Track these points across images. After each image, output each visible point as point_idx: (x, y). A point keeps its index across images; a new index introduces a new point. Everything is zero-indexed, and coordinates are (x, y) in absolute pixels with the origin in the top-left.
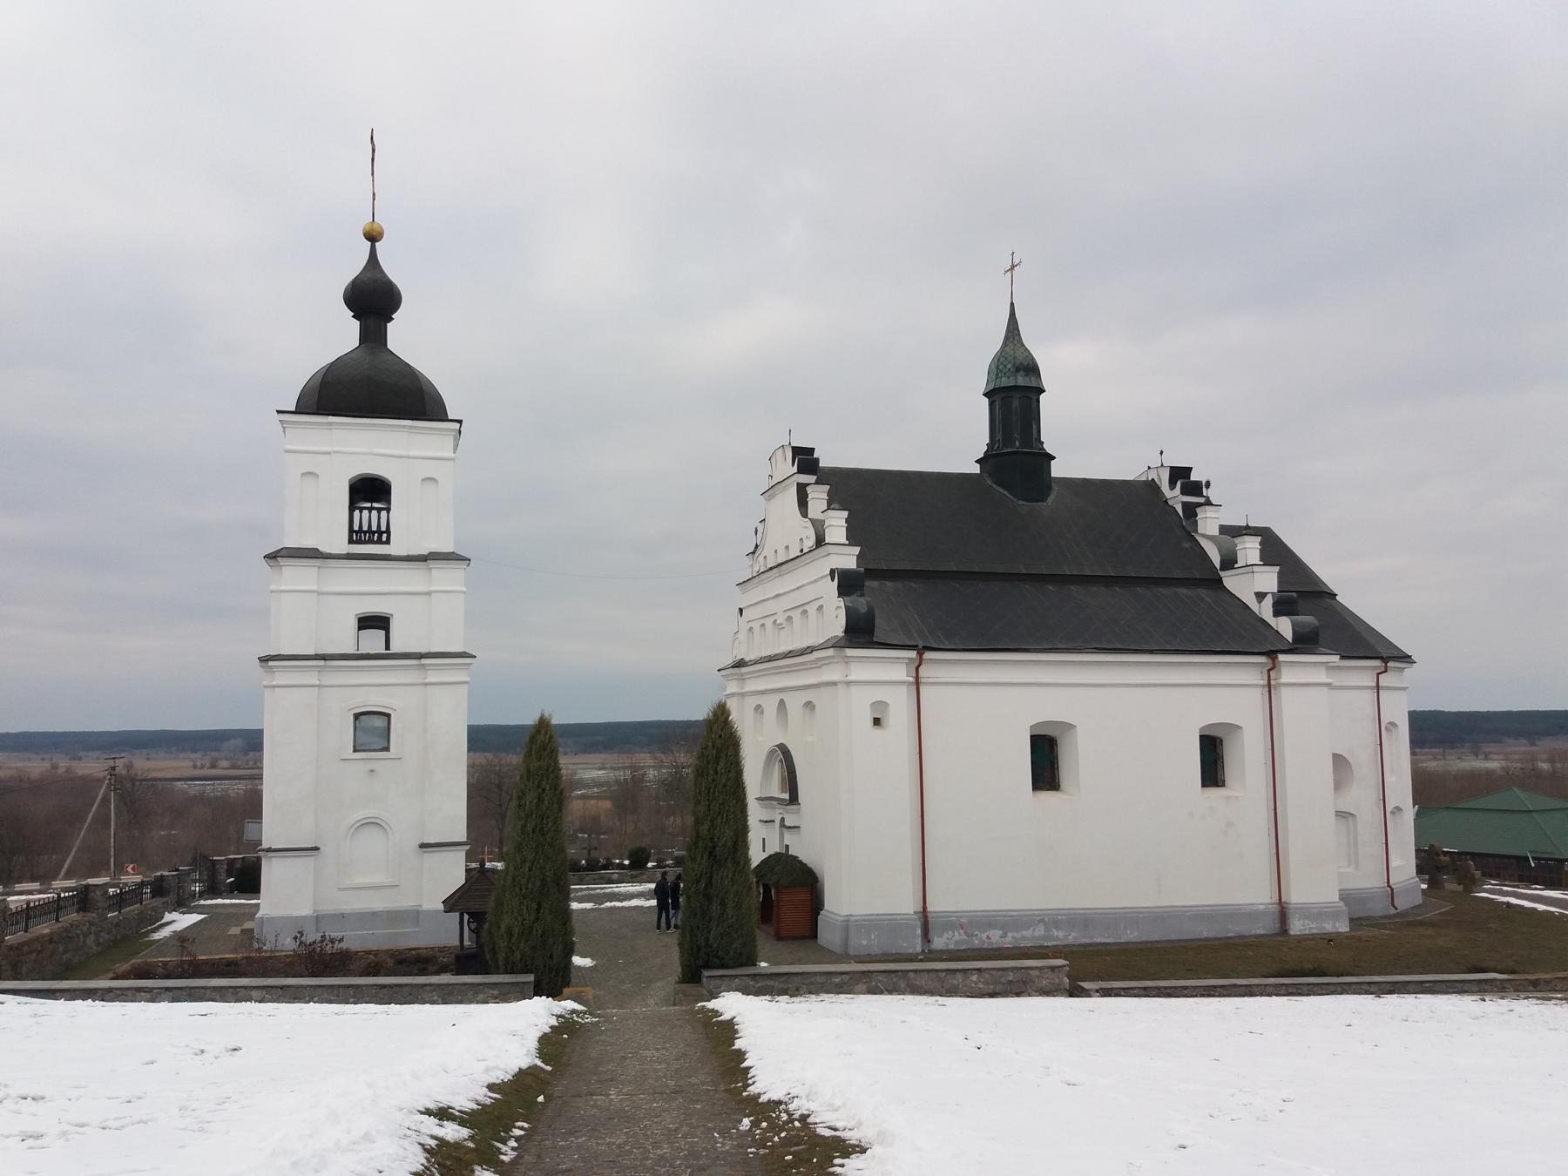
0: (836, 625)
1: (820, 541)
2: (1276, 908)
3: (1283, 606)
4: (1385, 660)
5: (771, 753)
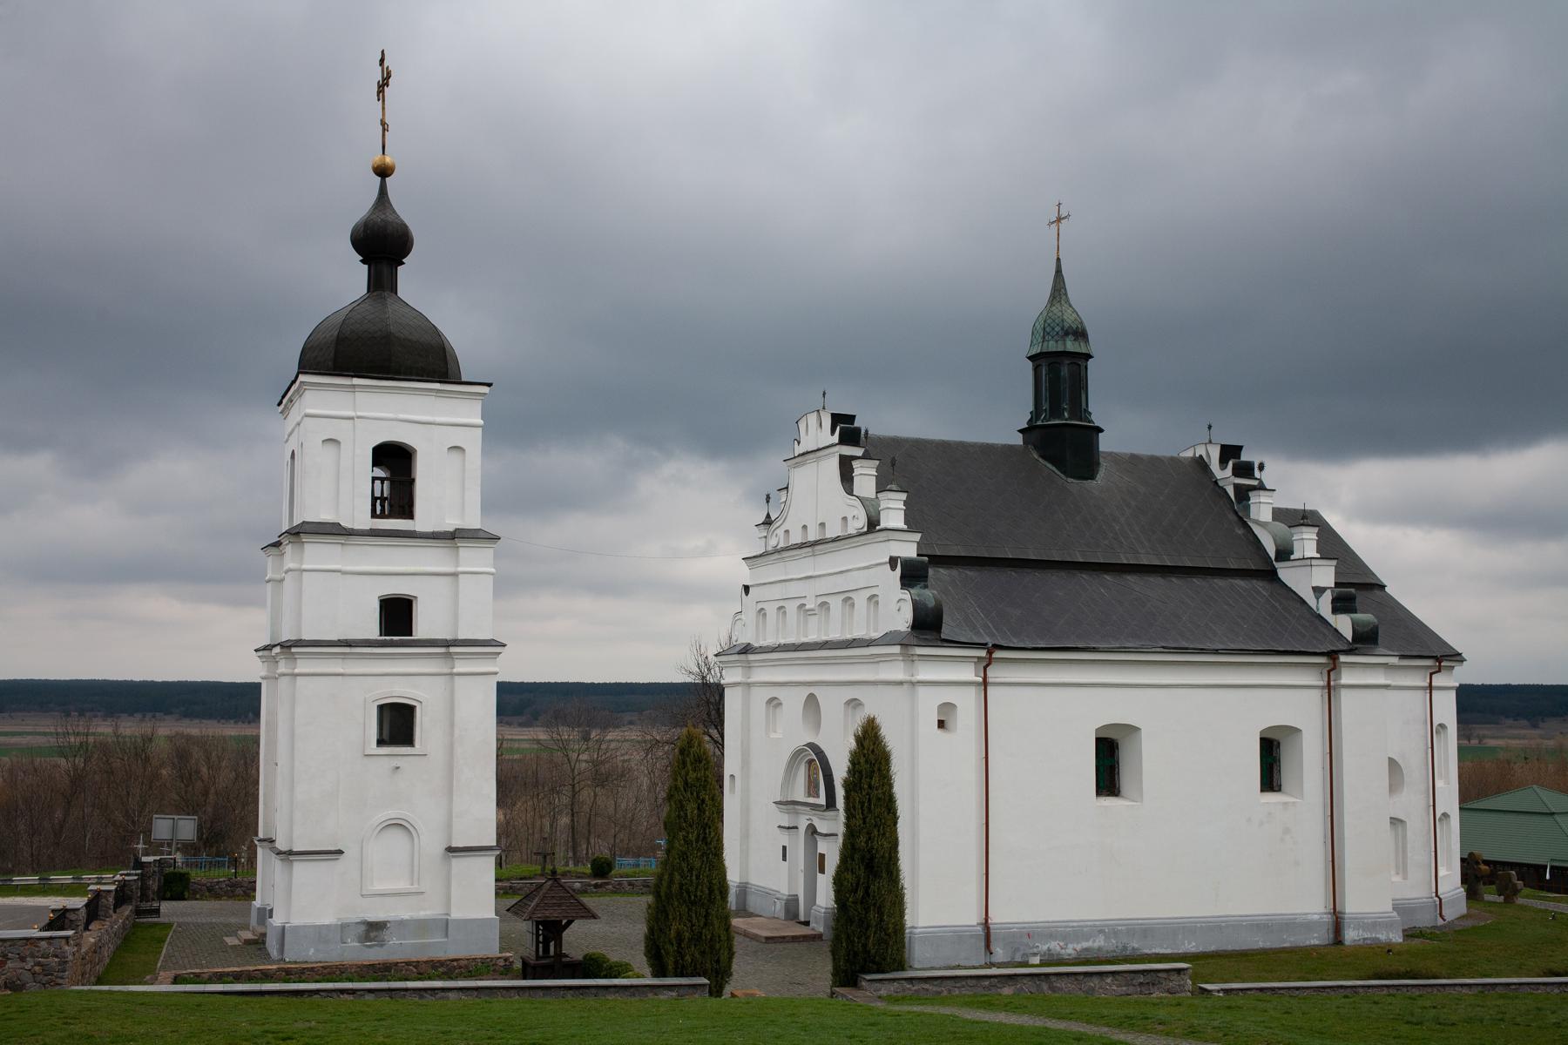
0: (902, 619)
1: (873, 524)
2: (1328, 918)
3: (1343, 603)
4: (1438, 659)
5: (798, 753)
